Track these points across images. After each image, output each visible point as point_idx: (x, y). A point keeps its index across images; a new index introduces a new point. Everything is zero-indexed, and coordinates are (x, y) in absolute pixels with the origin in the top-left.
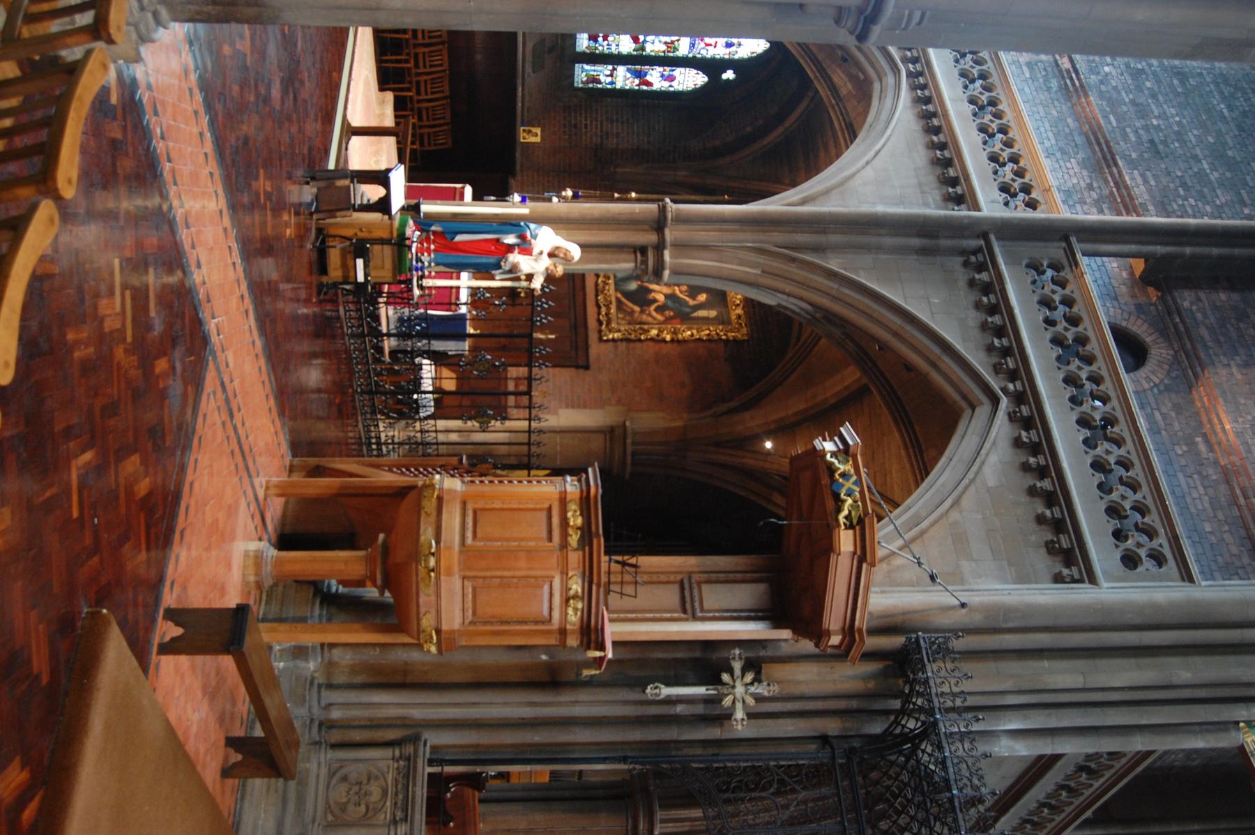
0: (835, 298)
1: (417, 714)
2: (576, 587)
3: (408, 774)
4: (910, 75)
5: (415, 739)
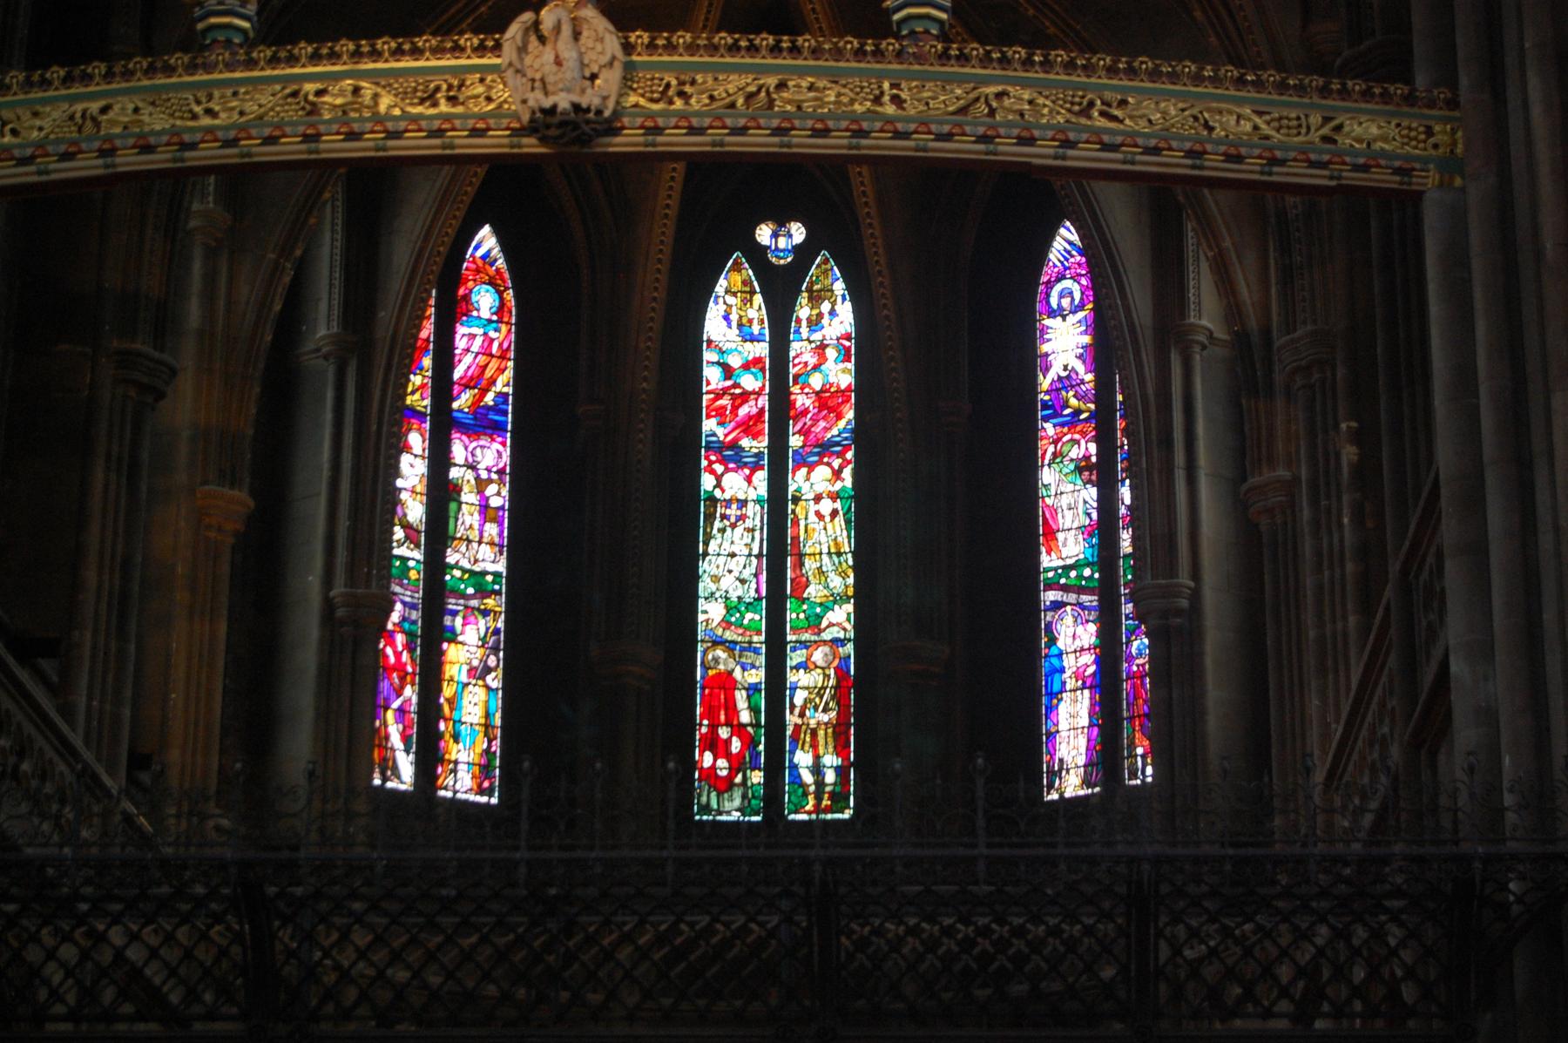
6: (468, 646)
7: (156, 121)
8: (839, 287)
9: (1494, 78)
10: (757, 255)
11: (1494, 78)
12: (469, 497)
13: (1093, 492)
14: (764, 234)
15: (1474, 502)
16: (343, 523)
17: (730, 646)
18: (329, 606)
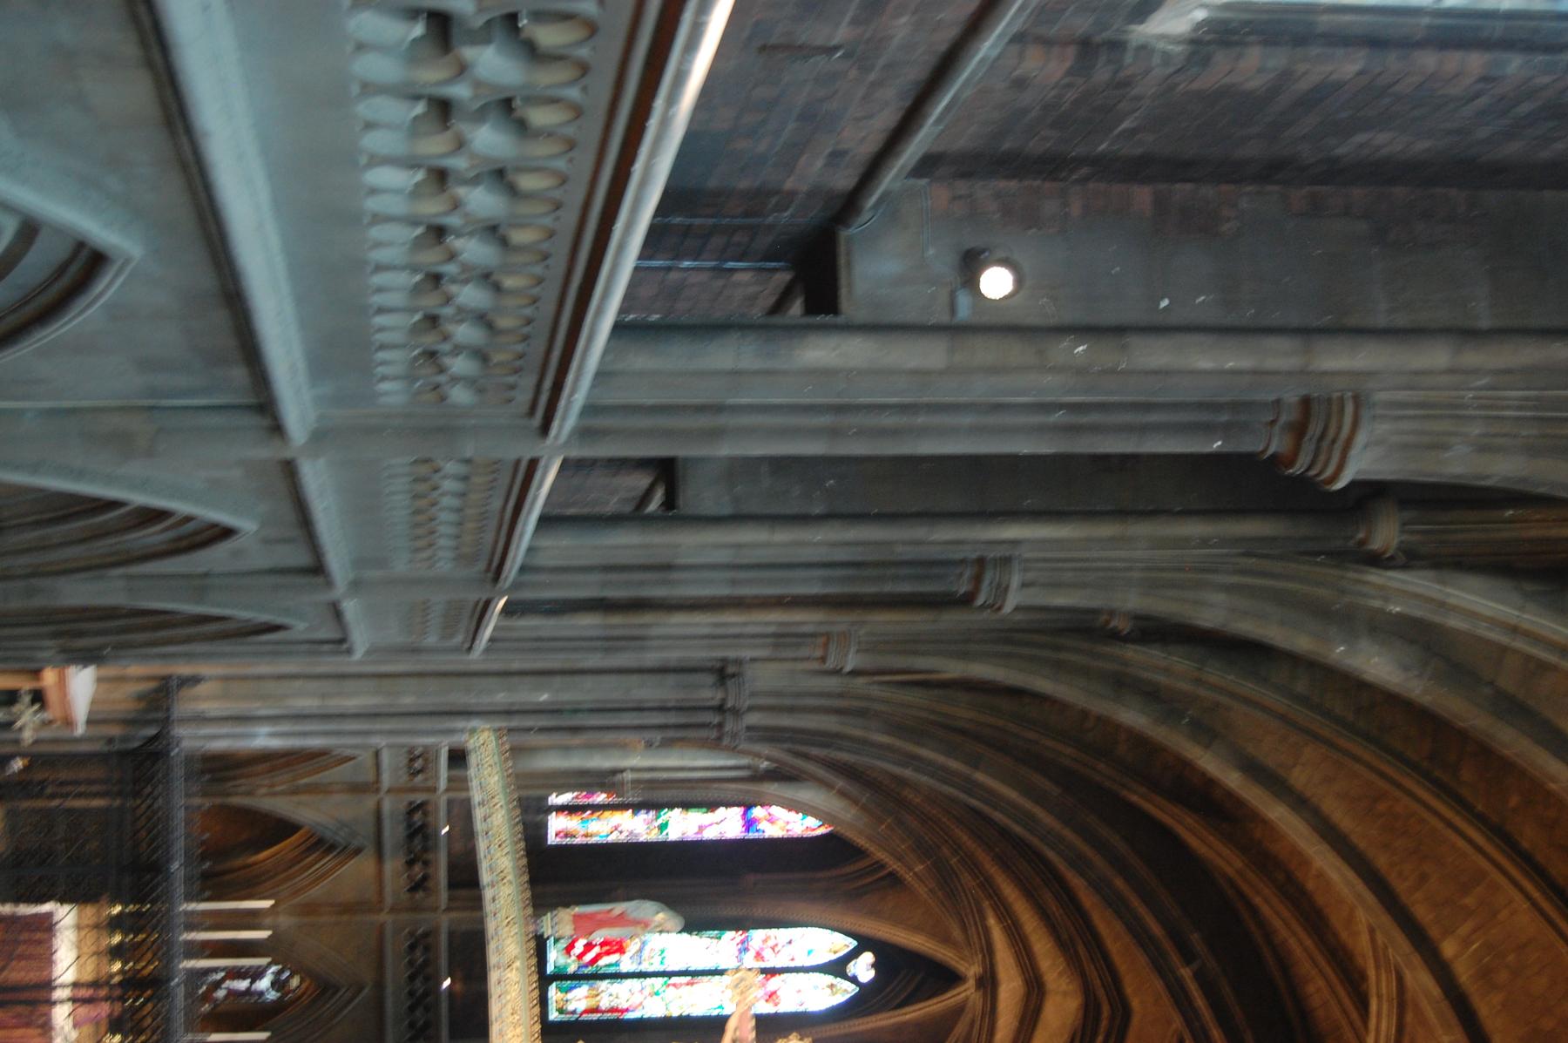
10: (853, 955)
14: (868, 958)
16: (665, 775)
17: (641, 950)
18: (622, 771)
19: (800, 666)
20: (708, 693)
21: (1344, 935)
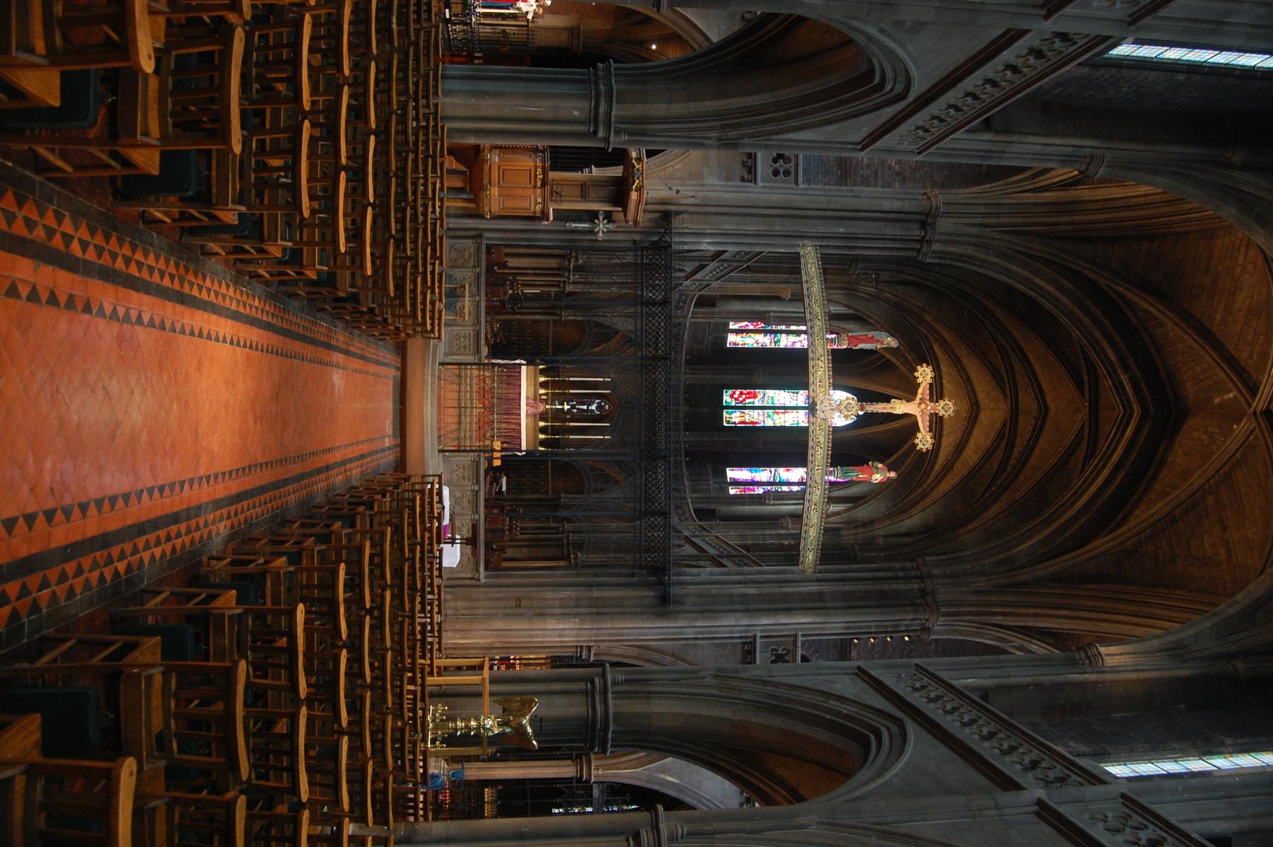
0: (674, 23)
1: (481, 226)
2: (539, 200)
3: (478, 249)
4: (548, 321)
5: (480, 236)
6: (764, 341)
7: (816, 329)
8: (849, 421)
9: (818, 580)
11: (818, 580)
12: (798, 339)
13: (796, 480)
15: (739, 573)
19: (961, 221)
20: (917, 232)
21: (1233, 352)
